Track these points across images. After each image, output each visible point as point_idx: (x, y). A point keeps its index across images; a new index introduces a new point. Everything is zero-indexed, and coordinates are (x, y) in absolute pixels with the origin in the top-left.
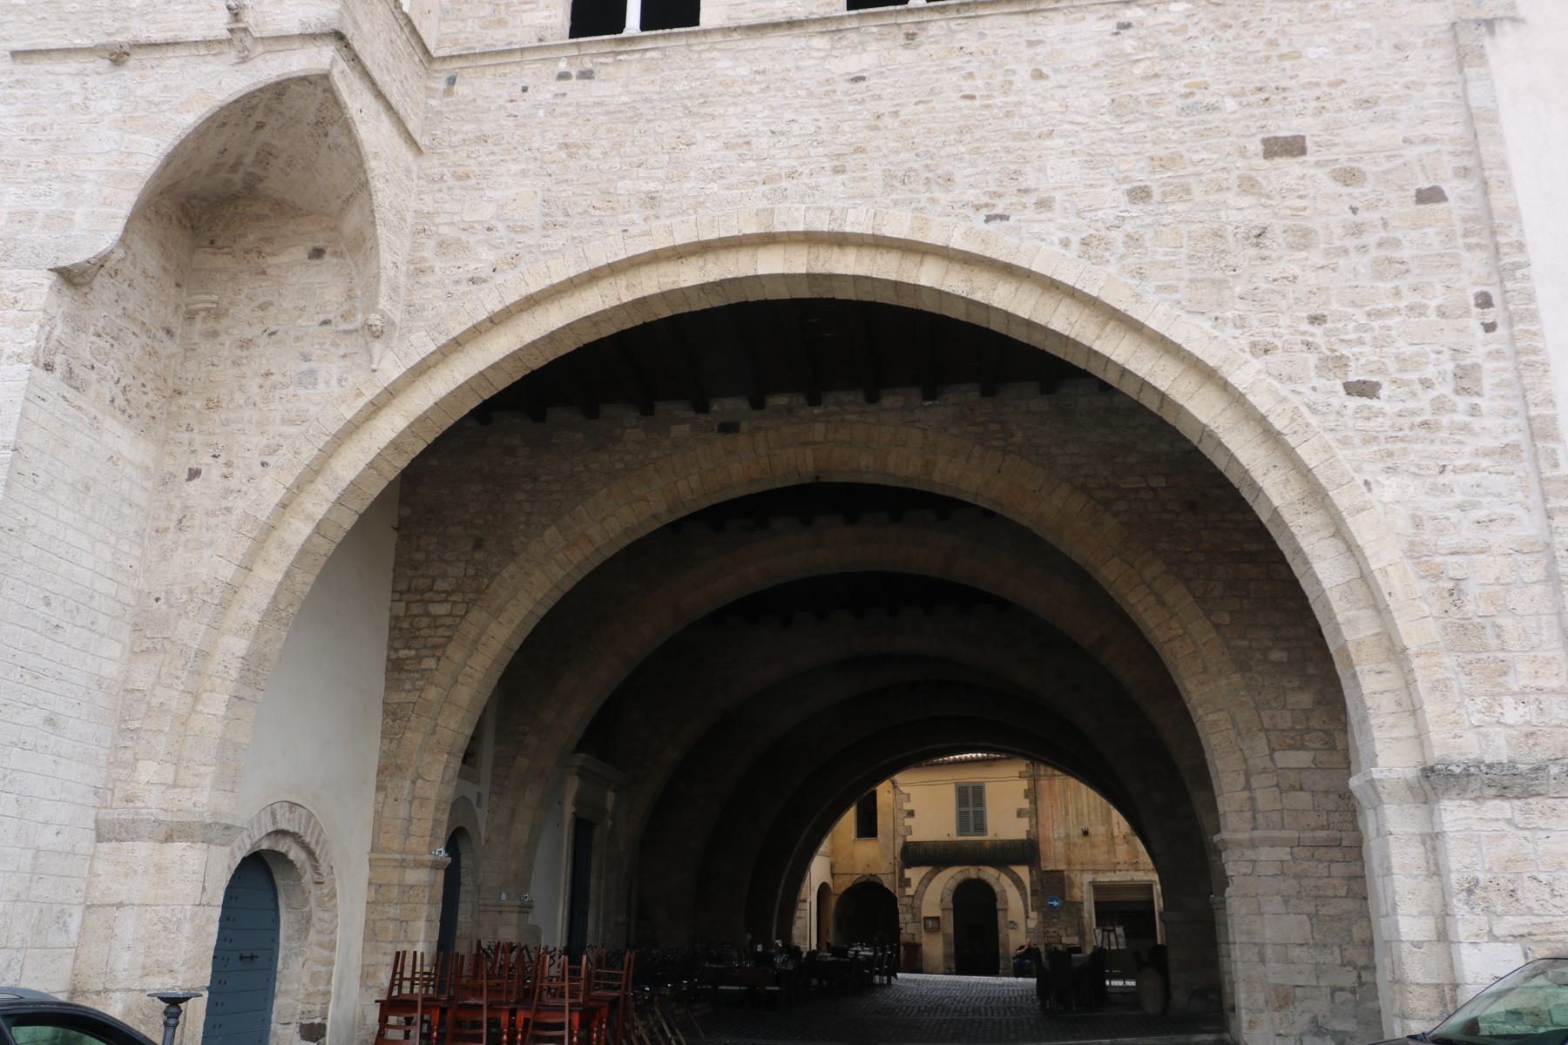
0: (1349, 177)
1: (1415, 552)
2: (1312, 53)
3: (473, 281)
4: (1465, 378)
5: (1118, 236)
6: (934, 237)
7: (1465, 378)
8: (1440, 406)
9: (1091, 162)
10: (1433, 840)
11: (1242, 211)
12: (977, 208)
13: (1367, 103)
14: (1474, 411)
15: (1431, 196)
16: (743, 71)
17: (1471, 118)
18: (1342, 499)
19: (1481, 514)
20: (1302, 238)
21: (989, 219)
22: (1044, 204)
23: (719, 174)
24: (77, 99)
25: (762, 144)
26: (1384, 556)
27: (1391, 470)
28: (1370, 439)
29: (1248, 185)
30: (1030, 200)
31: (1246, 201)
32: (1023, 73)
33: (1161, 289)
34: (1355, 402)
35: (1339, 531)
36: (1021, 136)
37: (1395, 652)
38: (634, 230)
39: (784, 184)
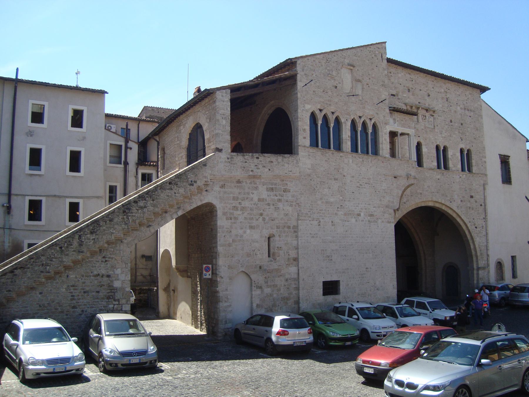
0: (476, 202)
1: (479, 245)
2: (474, 185)
3: (404, 203)
4: (483, 227)
5: (460, 206)
6: (446, 204)
7: (483, 227)
8: (481, 230)
9: (458, 196)
10: (478, 274)
11: (469, 205)
12: (449, 200)
13: (477, 192)
14: (483, 231)
15: (481, 205)
16: (428, 175)
17: (484, 197)
18: (475, 240)
19: (483, 242)
20: (473, 209)
21: (450, 202)
22: (454, 201)
23: (427, 191)
24: (392, 183)
25: (431, 187)
26: (477, 246)
27: (478, 237)
28: (476, 233)
29: (469, 201)
30: (453, 200)
31: (469, 203)
32: (452, 183)
33: (463, 214)
34: (476, 229)
35: (473, 242)
36: (452, 191)
37: (477, 256)
38: (420, 198)
39: (433, 194)
